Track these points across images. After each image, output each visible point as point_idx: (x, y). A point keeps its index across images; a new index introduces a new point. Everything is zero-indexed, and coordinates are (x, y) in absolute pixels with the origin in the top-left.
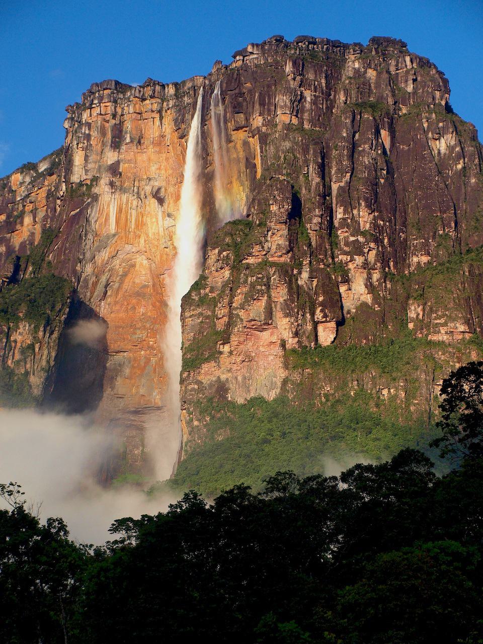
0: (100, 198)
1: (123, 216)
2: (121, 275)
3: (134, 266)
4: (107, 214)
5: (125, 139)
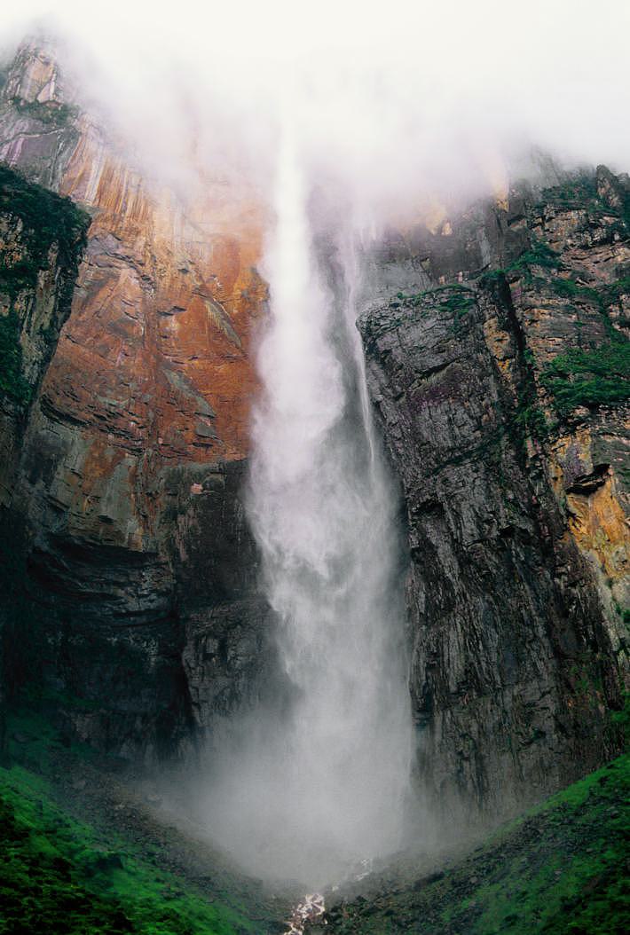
4: (85, 170)
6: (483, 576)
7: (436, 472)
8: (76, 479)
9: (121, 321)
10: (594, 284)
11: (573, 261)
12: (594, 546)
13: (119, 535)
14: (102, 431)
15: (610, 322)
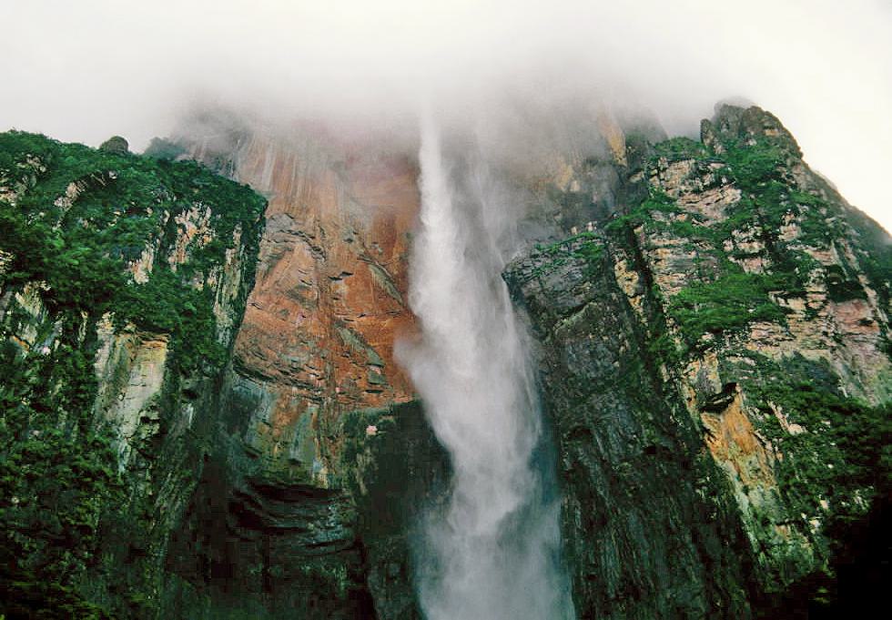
6: (631, 492)
7: (583, 400)
8: (267, 428)
9: (301, 287)
10: (708, 224)
11: (688, 205)
12: (729, 457)
13: (306, 475)
14: (287, 384)
15: (727, 255)
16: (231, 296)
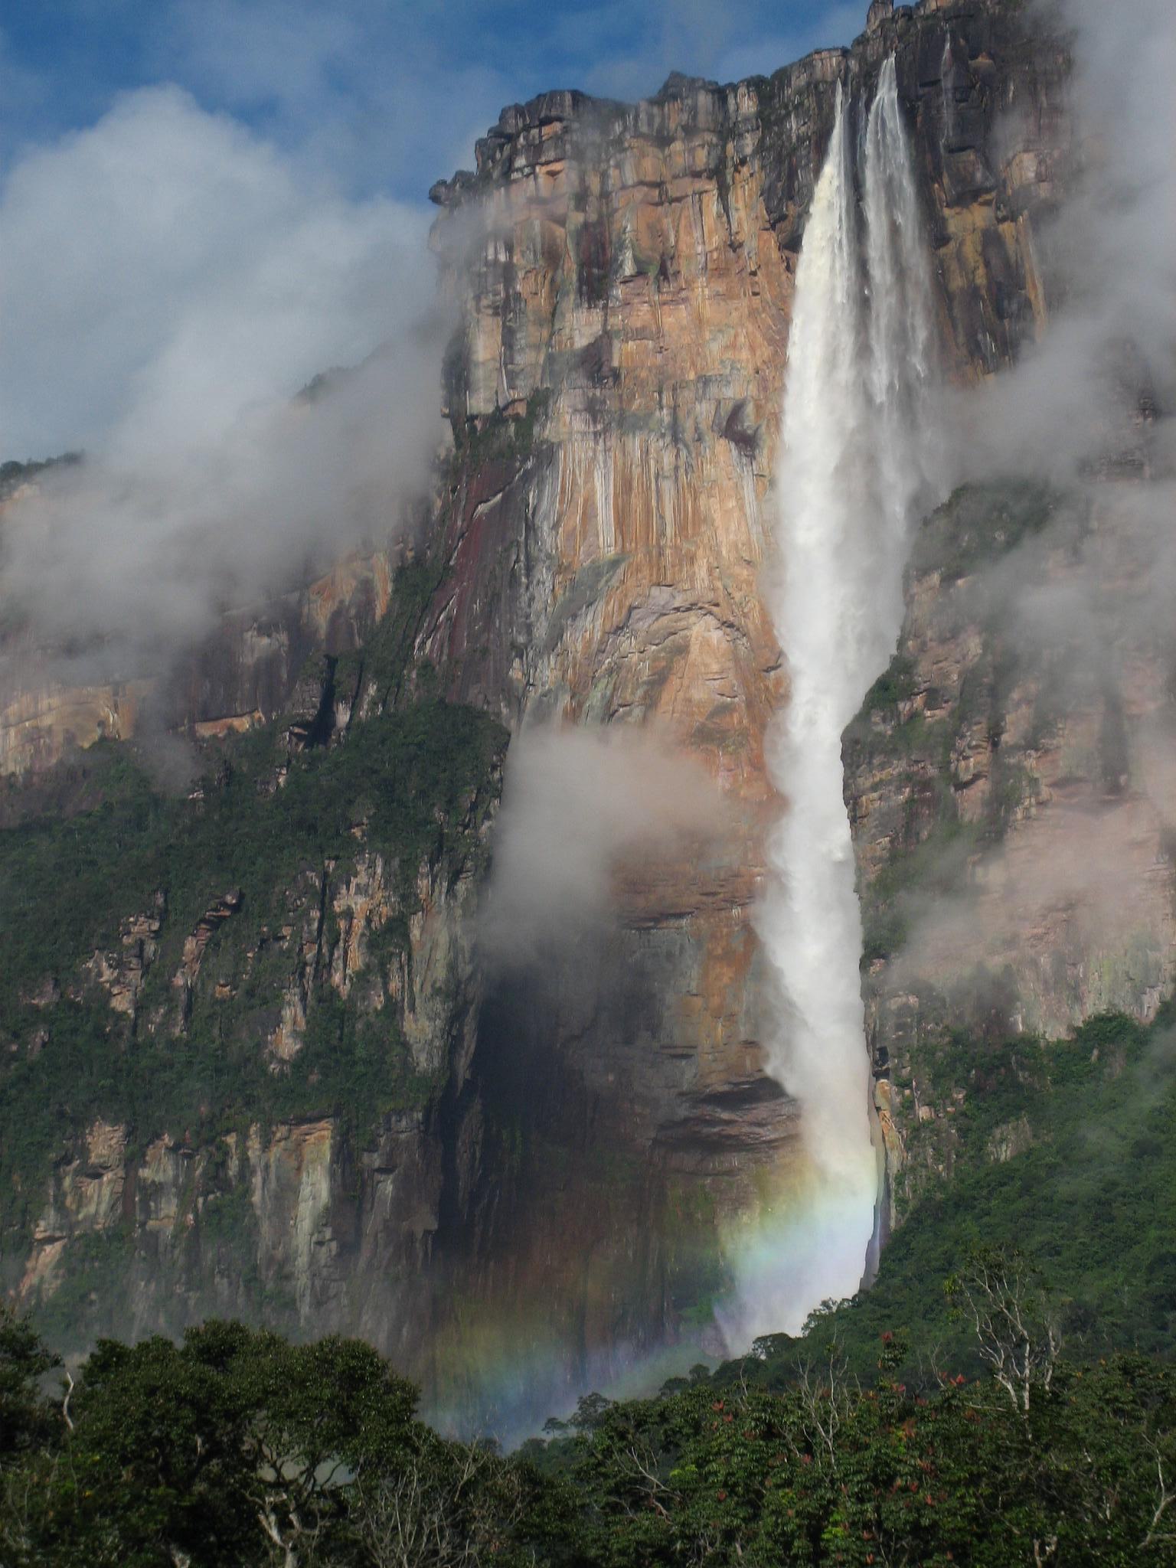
0: (561, 454)
1: (637, 502)
2: (648, 683)
3: (683, 650)
4: (586, 501)
5: (621, 266)
16: (435, 982)
